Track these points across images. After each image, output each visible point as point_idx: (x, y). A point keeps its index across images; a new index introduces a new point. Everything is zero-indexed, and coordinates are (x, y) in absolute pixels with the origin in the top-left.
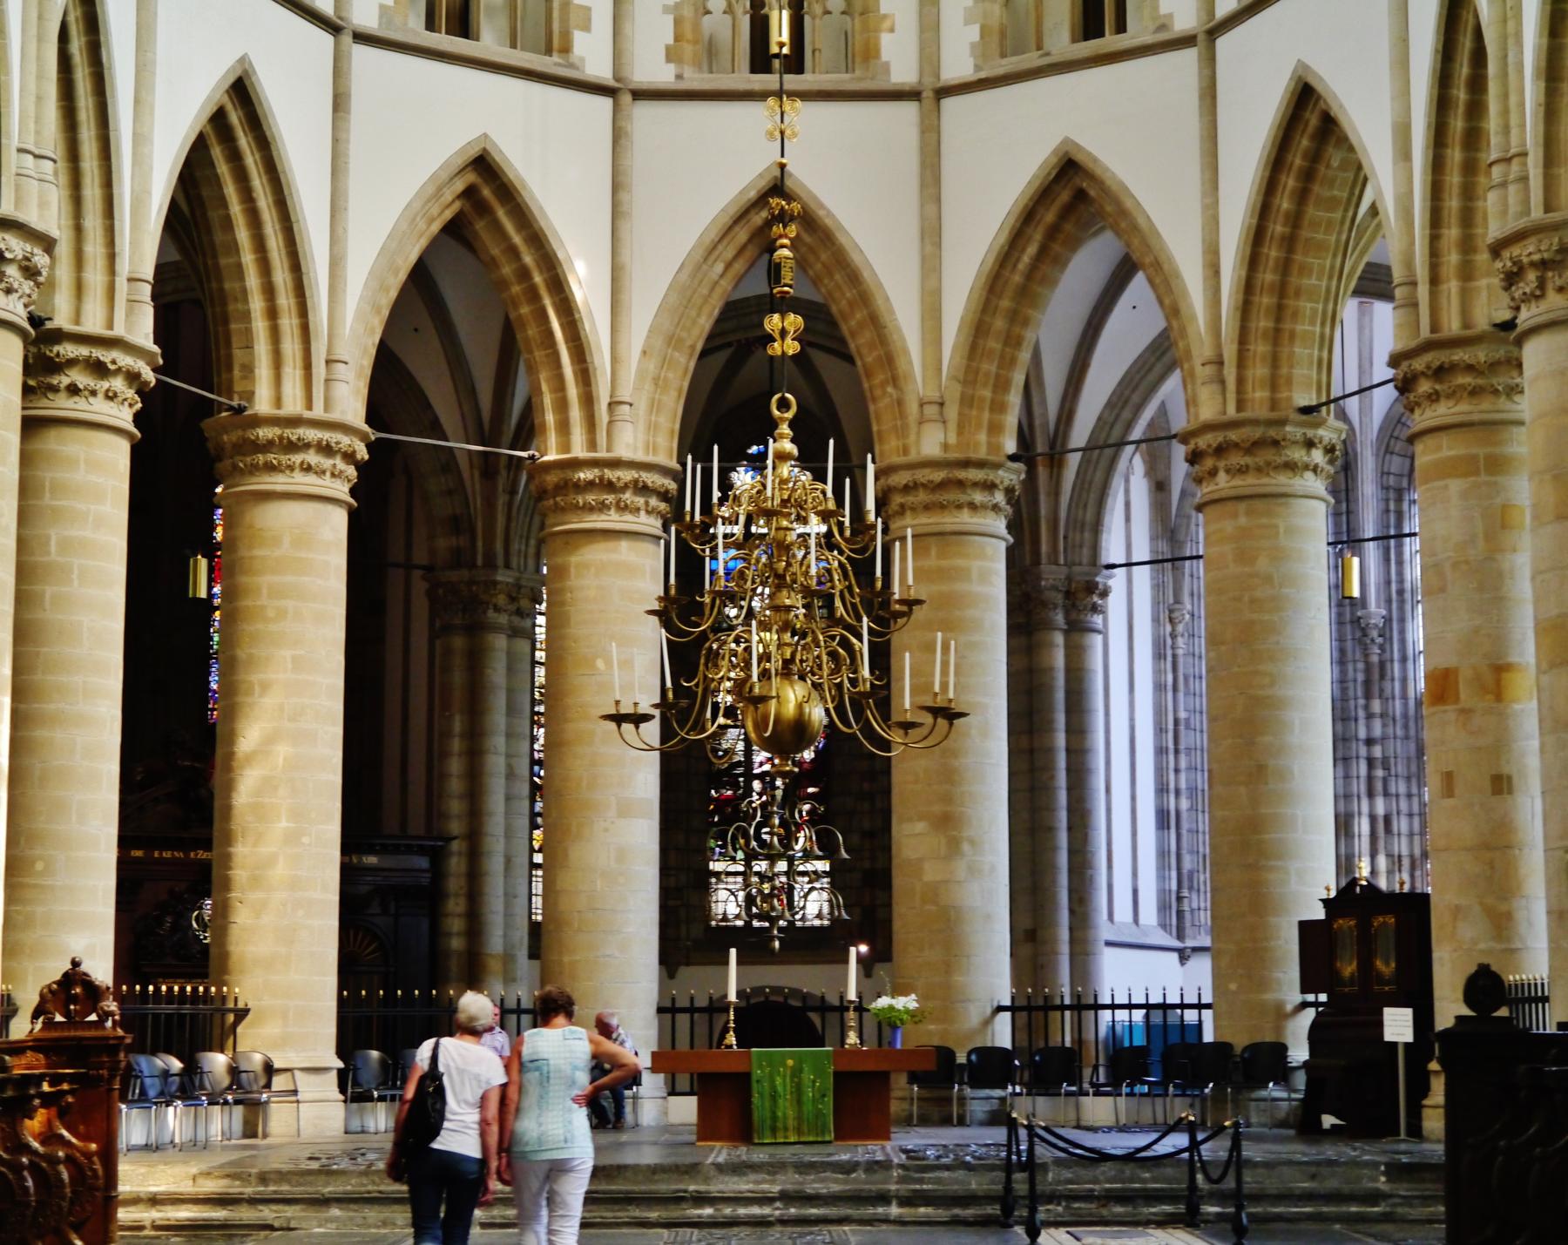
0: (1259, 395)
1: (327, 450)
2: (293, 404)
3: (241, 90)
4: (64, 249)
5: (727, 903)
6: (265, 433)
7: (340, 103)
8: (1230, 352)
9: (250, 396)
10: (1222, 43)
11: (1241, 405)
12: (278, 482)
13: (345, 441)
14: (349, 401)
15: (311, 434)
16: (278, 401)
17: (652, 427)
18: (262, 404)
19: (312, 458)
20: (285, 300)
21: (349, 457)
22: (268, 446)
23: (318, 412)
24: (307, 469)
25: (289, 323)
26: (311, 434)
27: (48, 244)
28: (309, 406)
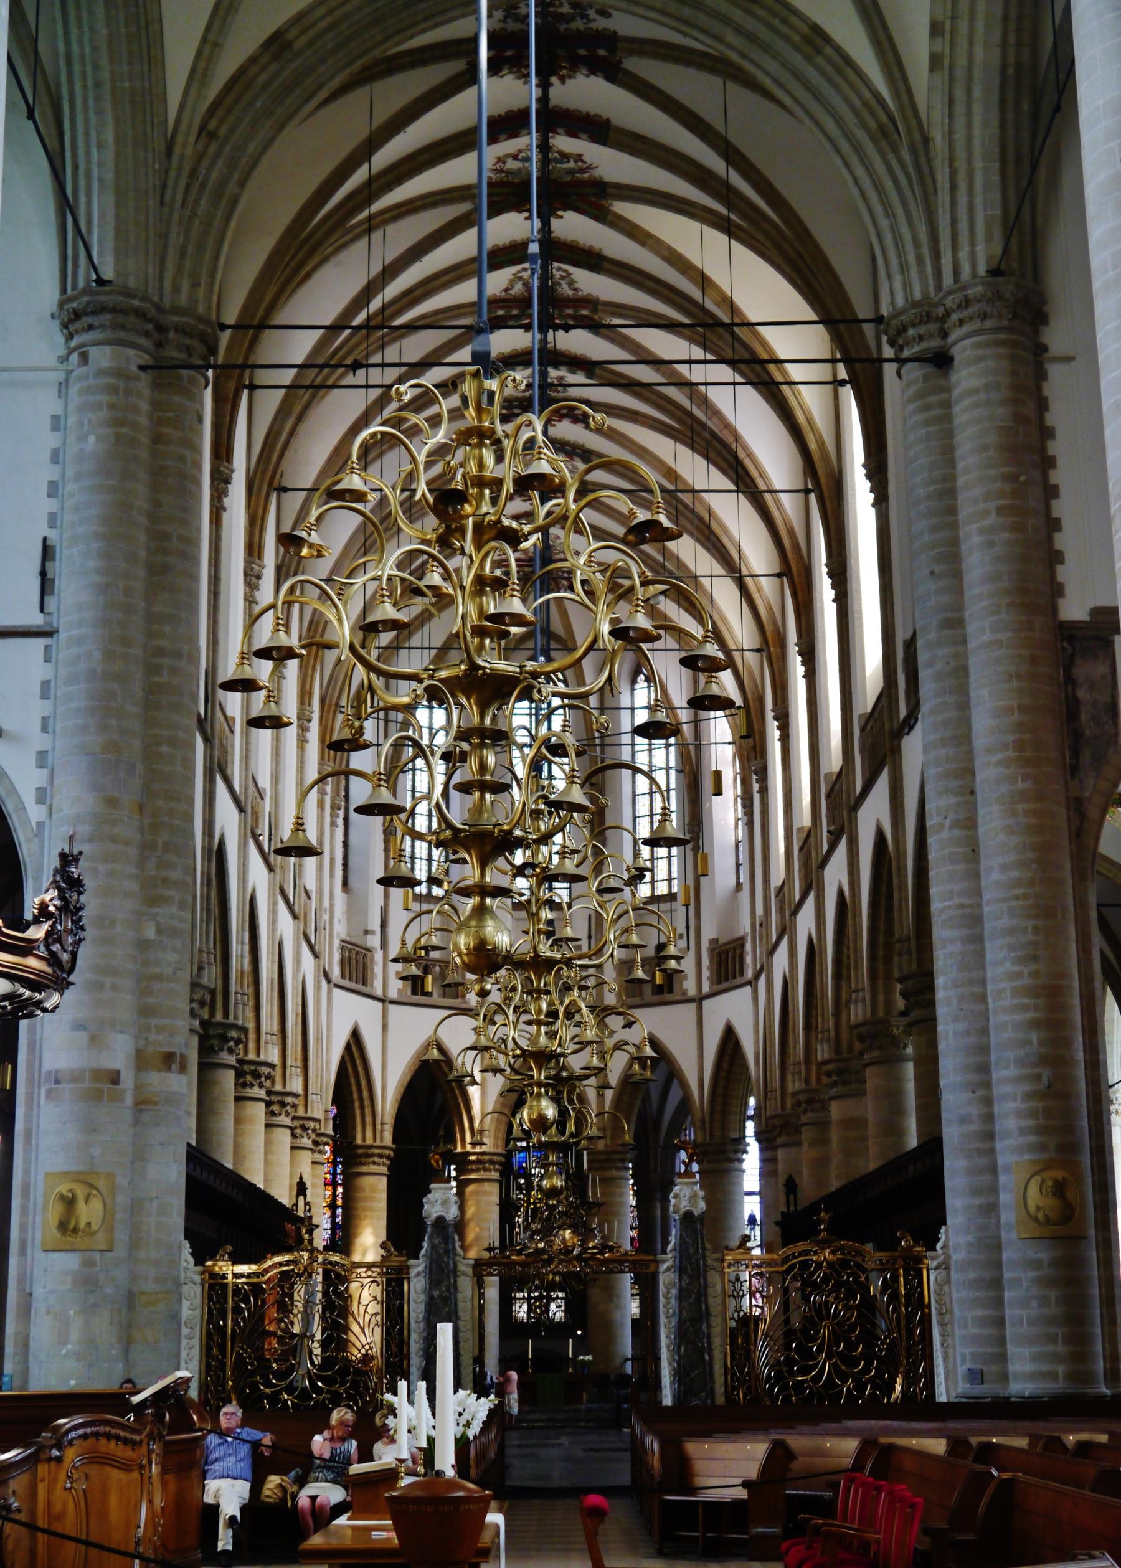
0: (718, 1134)
1: (381, 1156)
2: (369, 1141)
3: (355, 1035)
4: (279, 1070)
5: (521, 1311)
6: (360, 1151)
7: (385, 1028)
8: (707, 1117)
9: (354, 1137)
10: (705, 1003)
11: (712, 1136)
12: (364, 1169)
13: (387, 1152)
14: (388, 1138)
15: (376, 1151)
16: (364, 1139)
17: (496, 1138)
18: (359, 1141)
19: (376, 1159)
20: (367, 1103)
21: (388, 1158)
22: (361, 1156)
23: (378, 1143)
24: (374, 1163)
25: (368, 1111)
26: (376, 1151)
27: (296, 1096)
28: (375, 1139)
